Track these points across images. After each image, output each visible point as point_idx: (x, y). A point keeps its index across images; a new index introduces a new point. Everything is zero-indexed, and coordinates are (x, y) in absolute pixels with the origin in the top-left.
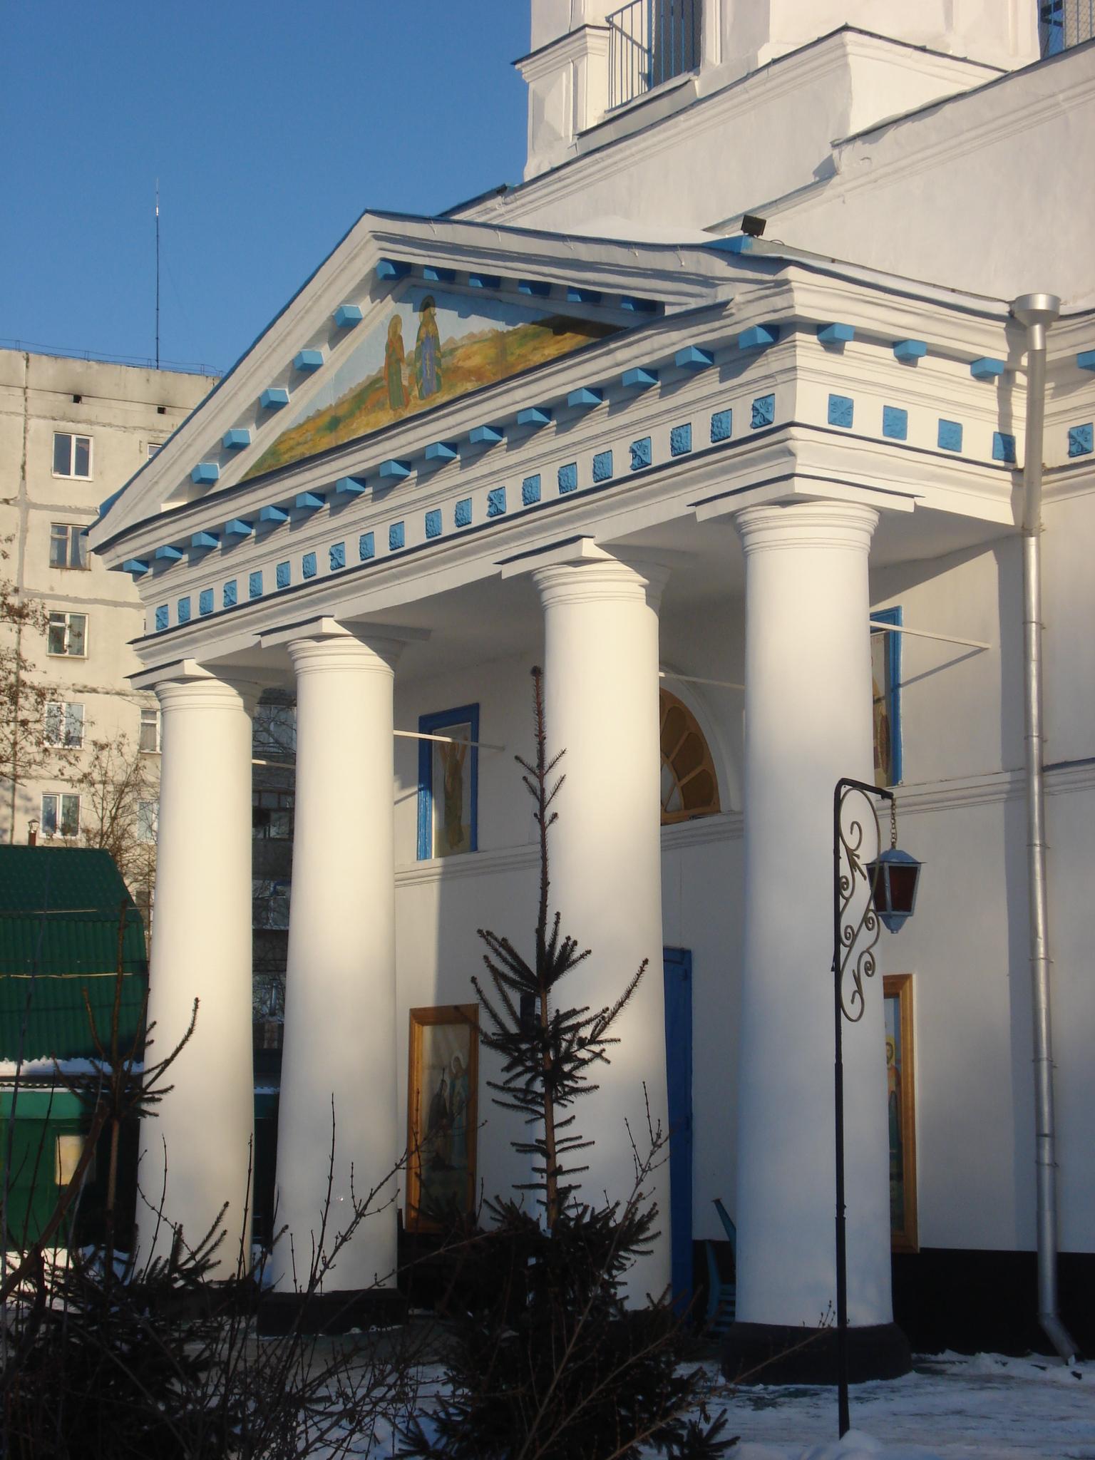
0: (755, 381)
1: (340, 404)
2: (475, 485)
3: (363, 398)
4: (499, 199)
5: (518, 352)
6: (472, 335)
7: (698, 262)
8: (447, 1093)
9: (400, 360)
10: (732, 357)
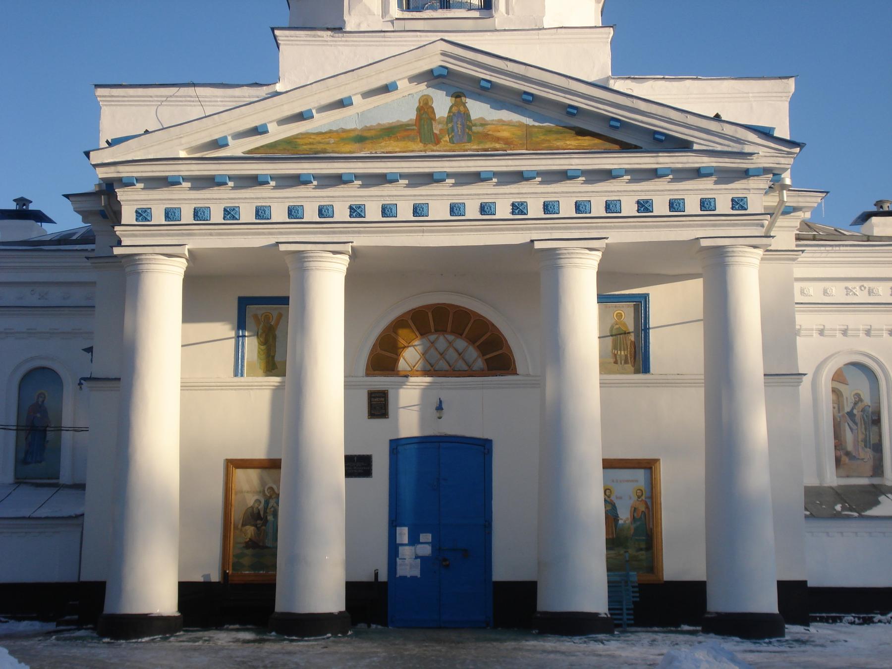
0: (737, 189)
1: (369, 129)
2: (500, 196)
3: (391, 132)
4: (329, 33)
5: (543, 137)
6: (500, 121)
7: (736, 131)
8: (261, 507)
9: (434, 119)
10: (726, 176)
